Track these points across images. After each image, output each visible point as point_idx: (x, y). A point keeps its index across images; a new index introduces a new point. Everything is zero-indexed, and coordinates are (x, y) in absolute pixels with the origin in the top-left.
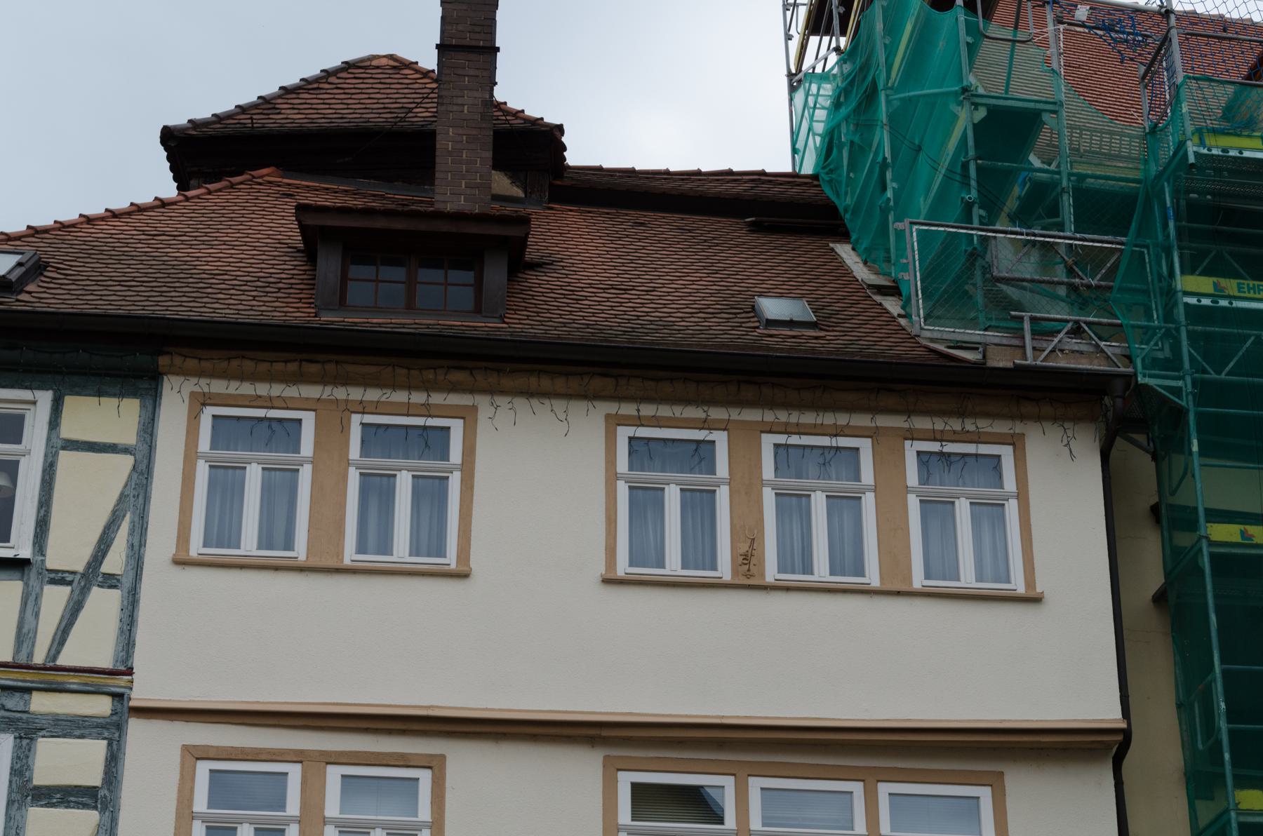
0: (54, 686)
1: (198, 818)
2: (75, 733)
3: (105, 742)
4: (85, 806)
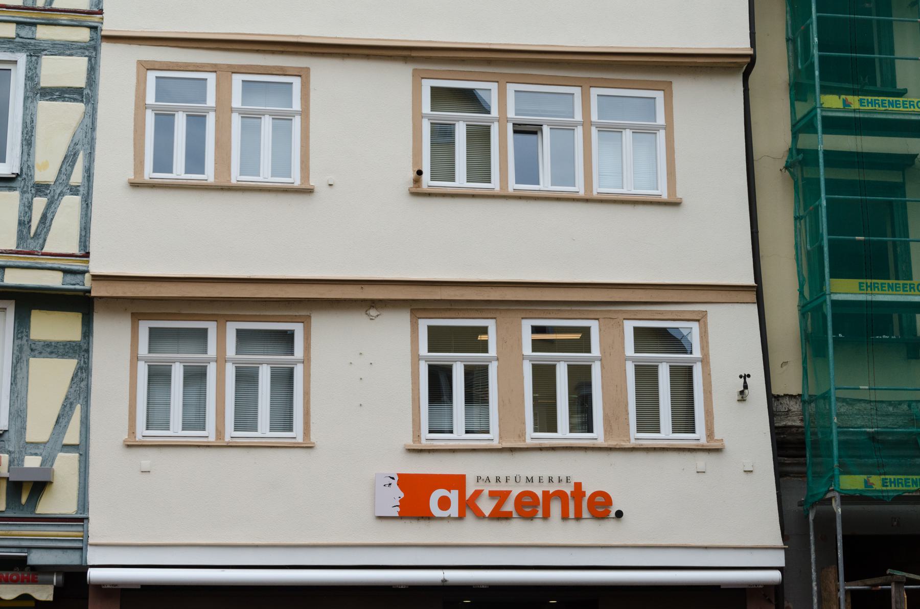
0: (51, 22)
1: (149, 108)
2: (67, 53)
3: (86, 59)
4: (75, 100)
